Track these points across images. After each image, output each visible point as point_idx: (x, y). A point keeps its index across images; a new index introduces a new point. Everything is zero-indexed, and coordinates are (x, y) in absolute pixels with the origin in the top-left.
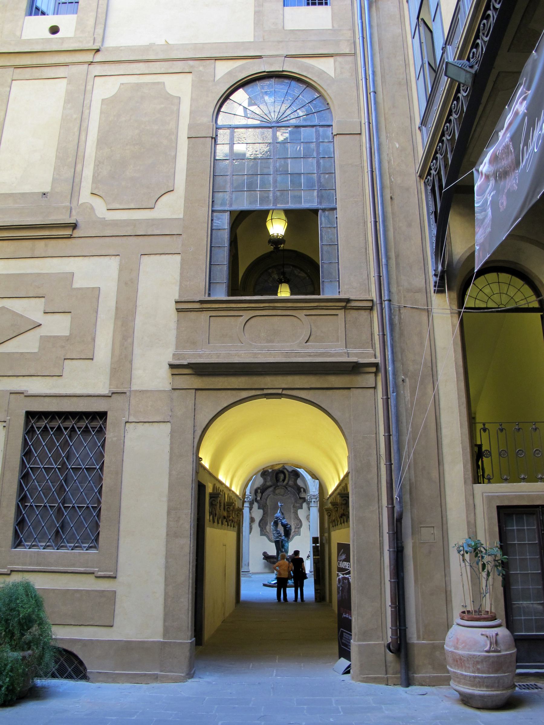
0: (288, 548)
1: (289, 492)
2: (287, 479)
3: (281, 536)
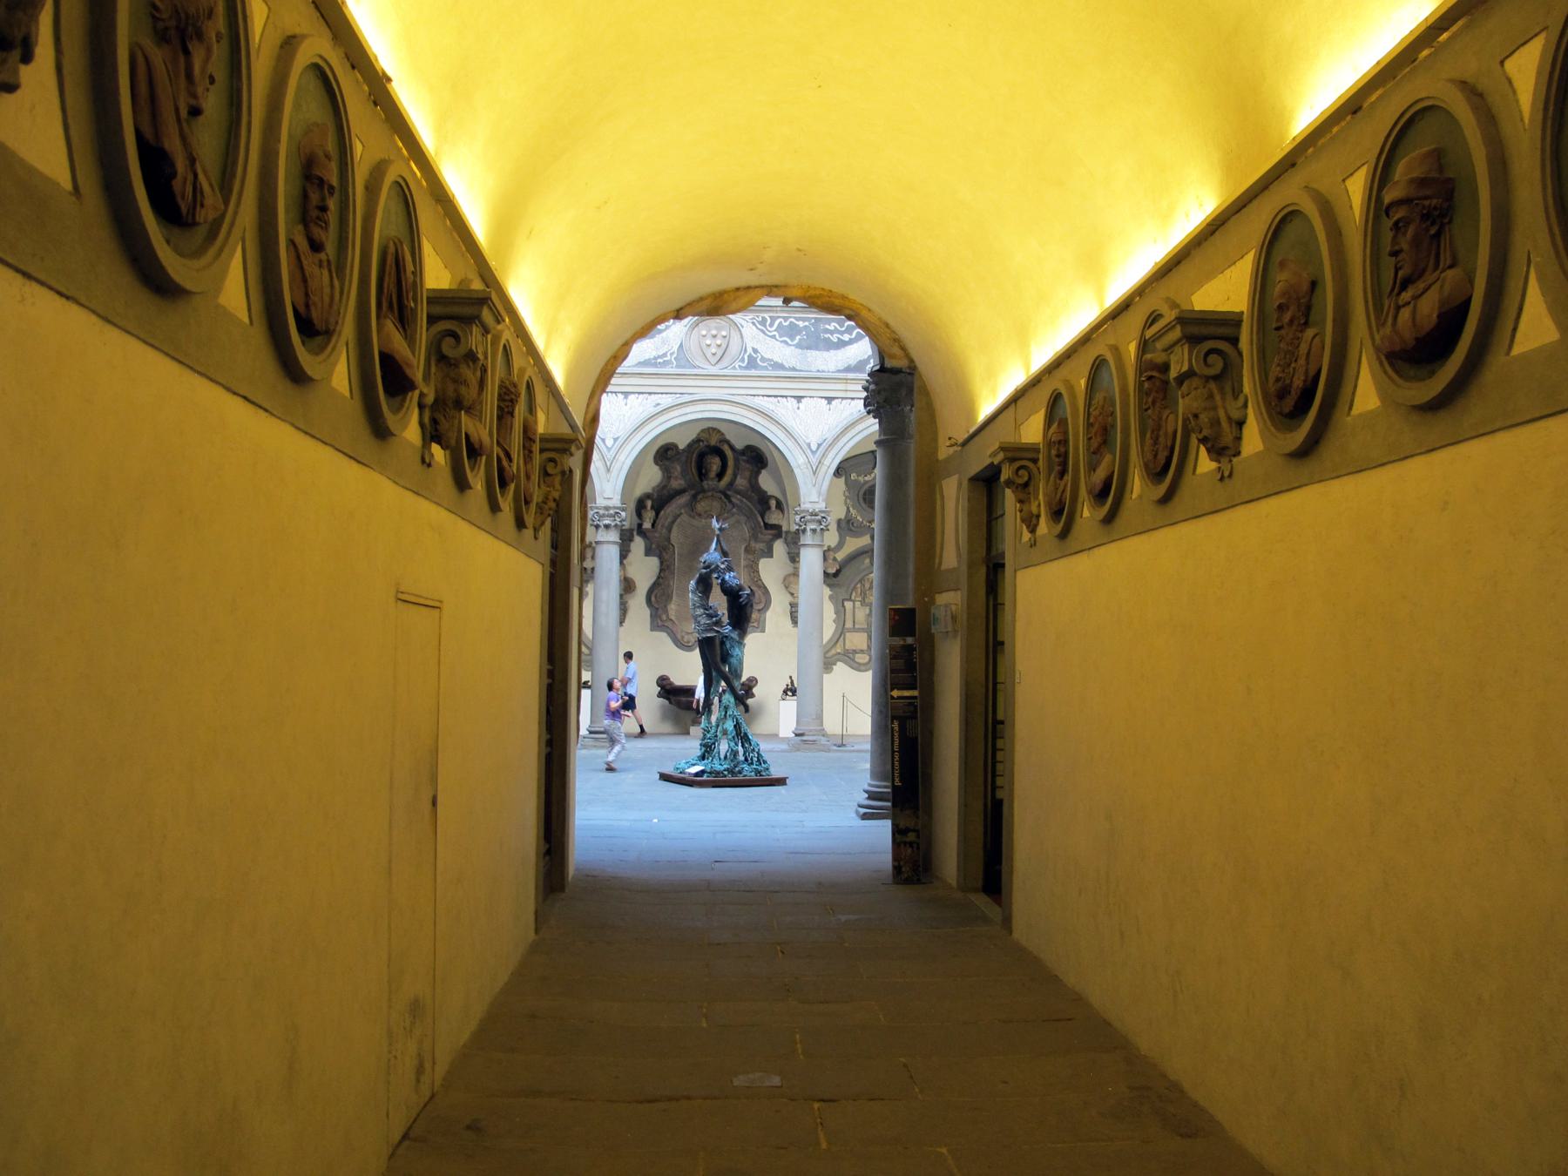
0: (741, 662)
1: (734, 510)
2: (730, 472)
3: (718, 623)
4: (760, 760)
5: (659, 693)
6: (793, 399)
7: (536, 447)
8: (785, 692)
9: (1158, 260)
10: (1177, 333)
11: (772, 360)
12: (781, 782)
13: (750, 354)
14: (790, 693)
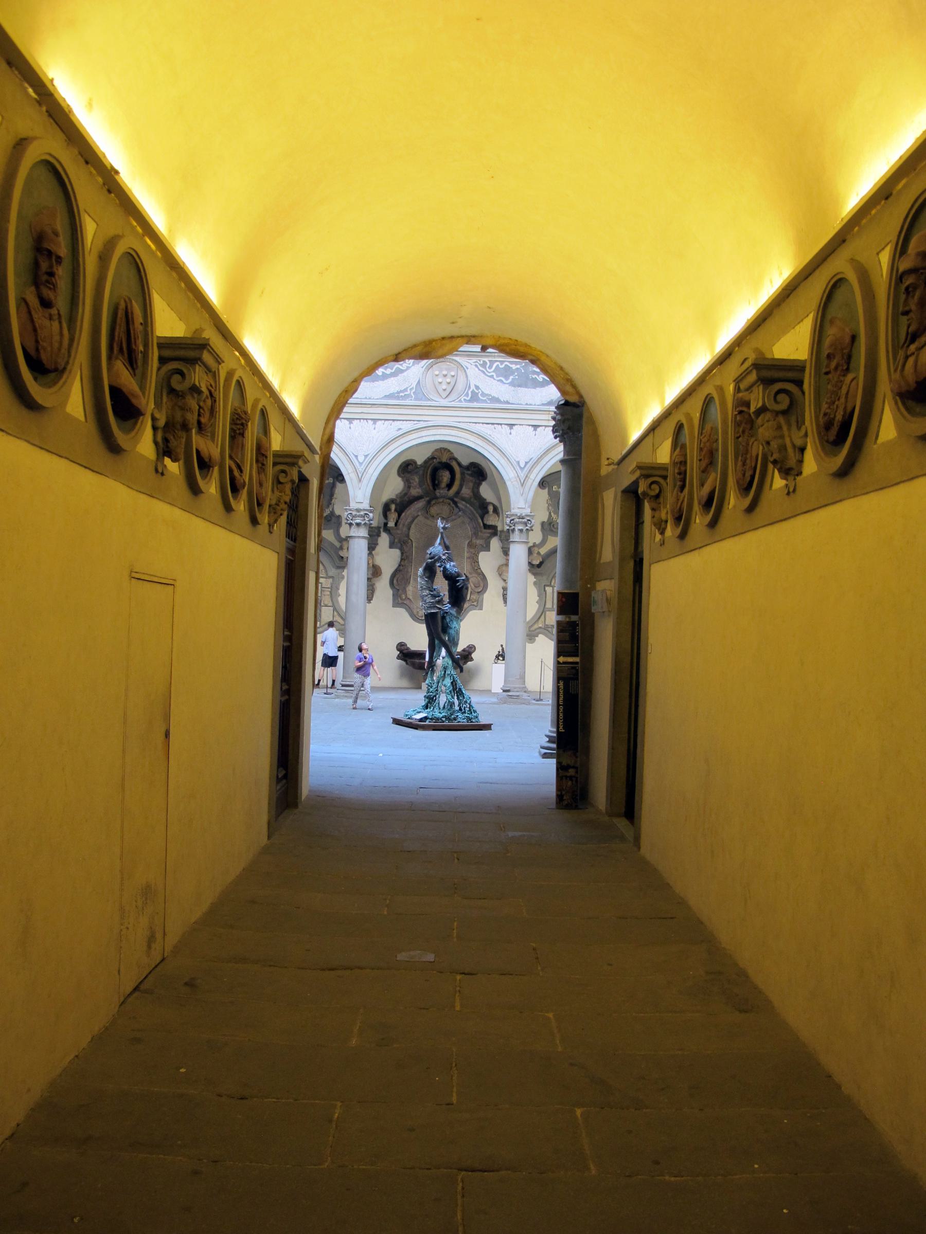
0: (458, 633)
1: (460, 513)
4: (471, 710)
5: (398, 656)
6: (506, 426)
7: (270, 461)
8: (497, 657)
9: (749, 318)
10: (753, 377)
11: (490, 395)
12: (487, 727)
13: (473, 390)
14: (501, 658)
